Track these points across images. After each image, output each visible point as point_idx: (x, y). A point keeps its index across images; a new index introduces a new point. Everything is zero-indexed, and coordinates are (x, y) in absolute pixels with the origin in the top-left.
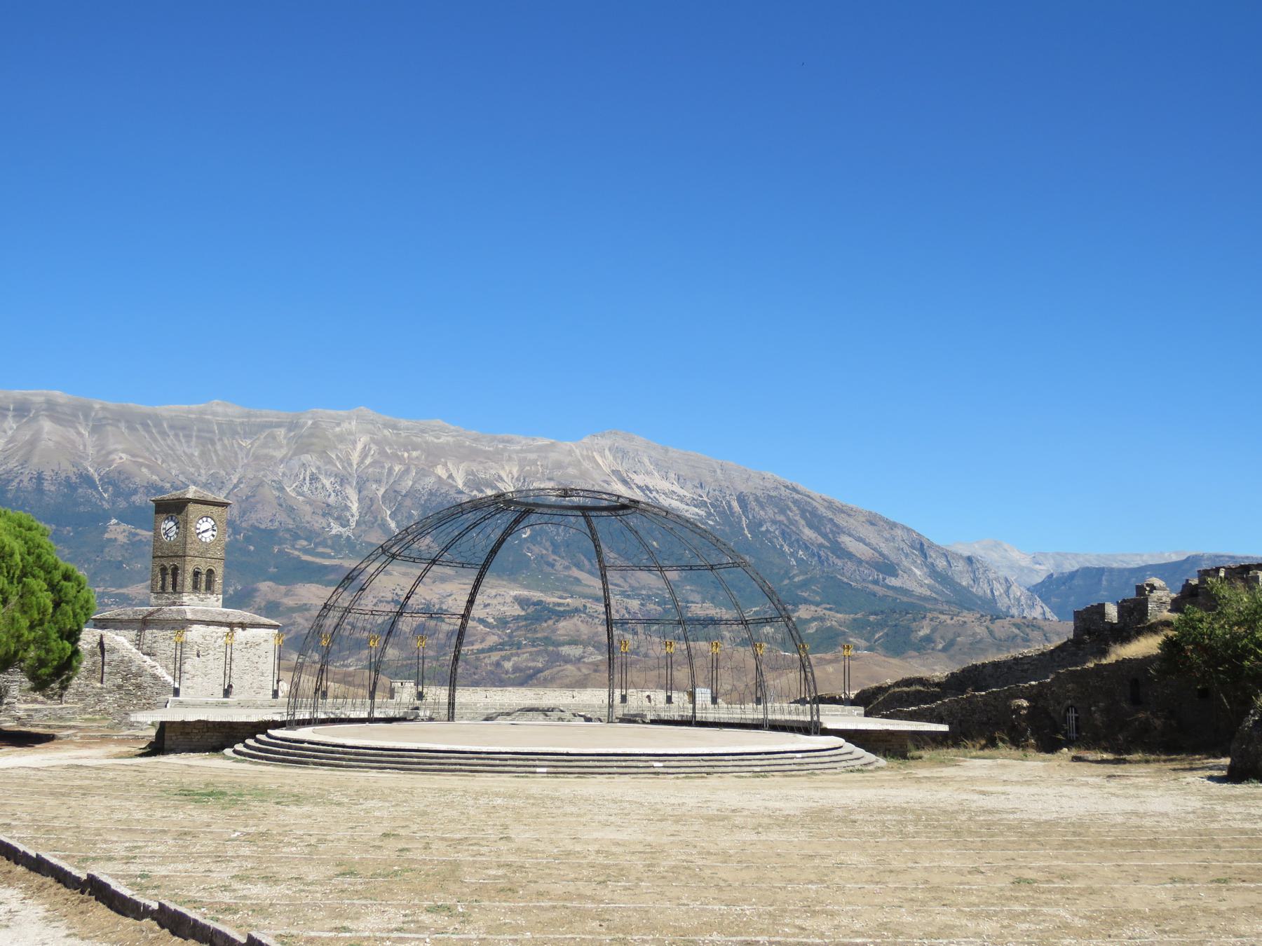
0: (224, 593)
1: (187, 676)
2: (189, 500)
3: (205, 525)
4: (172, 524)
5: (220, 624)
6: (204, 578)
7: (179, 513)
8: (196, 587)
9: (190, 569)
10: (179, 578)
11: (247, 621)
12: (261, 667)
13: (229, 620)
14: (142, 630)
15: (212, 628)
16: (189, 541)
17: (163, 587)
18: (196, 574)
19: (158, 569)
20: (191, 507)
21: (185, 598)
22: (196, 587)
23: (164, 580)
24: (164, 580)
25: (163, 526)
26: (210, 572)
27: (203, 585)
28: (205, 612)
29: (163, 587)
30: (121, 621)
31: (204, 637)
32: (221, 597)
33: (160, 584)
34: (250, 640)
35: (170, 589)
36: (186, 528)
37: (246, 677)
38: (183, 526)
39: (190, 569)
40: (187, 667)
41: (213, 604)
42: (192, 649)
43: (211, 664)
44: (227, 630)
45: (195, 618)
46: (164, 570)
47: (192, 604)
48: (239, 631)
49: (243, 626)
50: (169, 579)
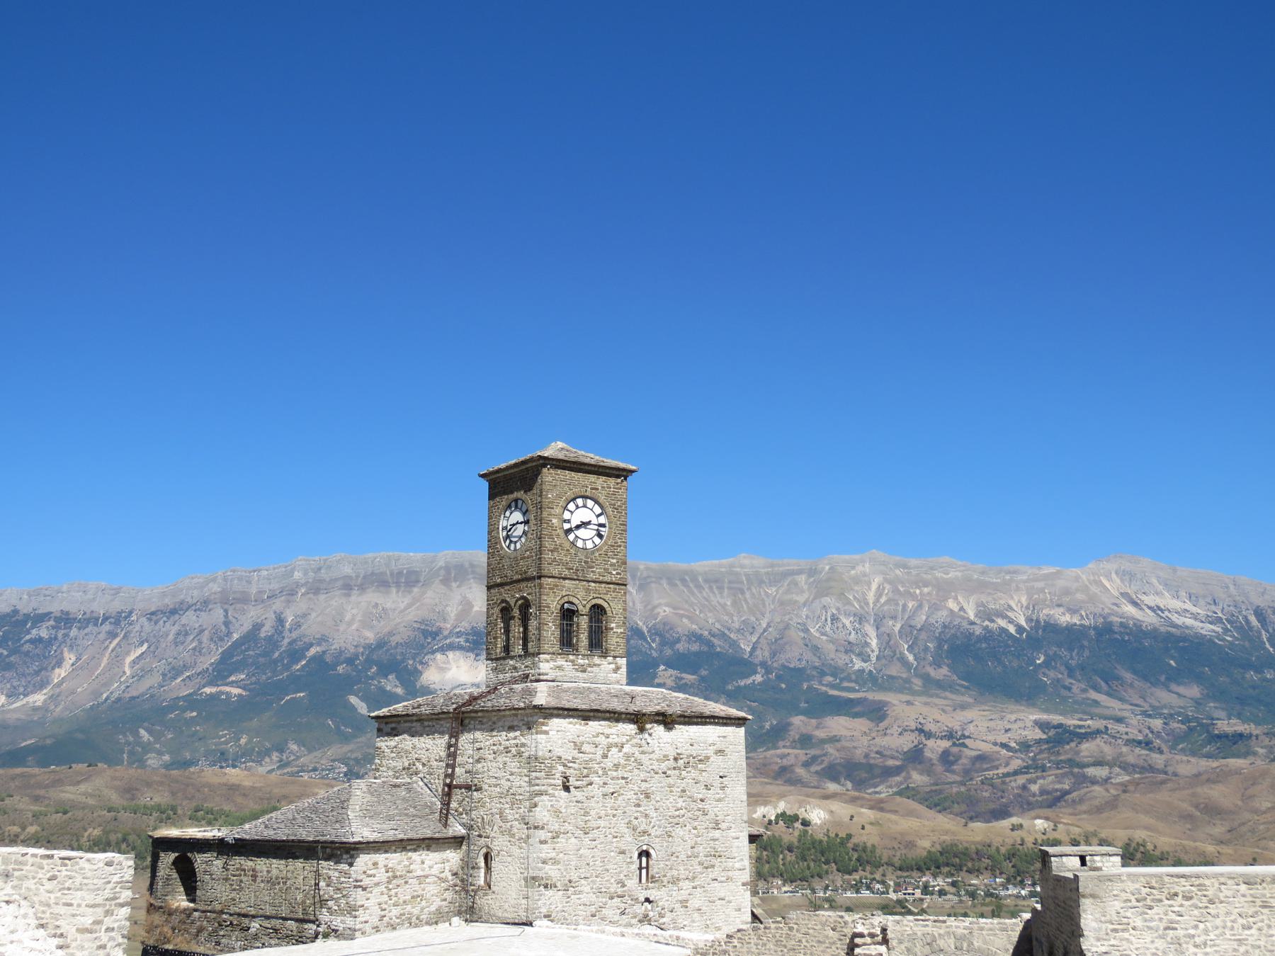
0: (628, 655)
1: (542, 834)
2: (545, 462)
3: (583, 513)
4: (517, 516)
5: (614, 716)
6: (584, 622)
7: (528, 489)
8: (567, 642)
9: (553, 603)
10: (533, 624)
11: (676, 709)
12: (714, 809)
13: (633, 708)
14: (455, 735)
15: (595, 726)
16: (548, 544)
17: (507, 649)
18: (568, 614)
19: (497, 610)
20: (548, 475)
21: (546, 666)
22: (567, 642)
23: (507, 631)
24: (507, 631)
25: (503, 523)
26: (598, 612)
27: (584, 638)
28: (581, 692)
29: (507, 649)
30: (420, 719)
31: (578, 747)
32: (623, 662)
33: (500, 644)
34: (685, 750)
35: (518, 649)
36: (540, 520)
37: (679, 831)
38: (536, 518)
39: (553, 603)
40: (541, 814)
41: (607, 677)
42: (549, 775)
43: (596, 807)
44: (631, 728)
45: (554, 703)
46: (506, 611)
47: (557, 675)
48: (659, 730)
49: (667, 720)
50: (517, 629)
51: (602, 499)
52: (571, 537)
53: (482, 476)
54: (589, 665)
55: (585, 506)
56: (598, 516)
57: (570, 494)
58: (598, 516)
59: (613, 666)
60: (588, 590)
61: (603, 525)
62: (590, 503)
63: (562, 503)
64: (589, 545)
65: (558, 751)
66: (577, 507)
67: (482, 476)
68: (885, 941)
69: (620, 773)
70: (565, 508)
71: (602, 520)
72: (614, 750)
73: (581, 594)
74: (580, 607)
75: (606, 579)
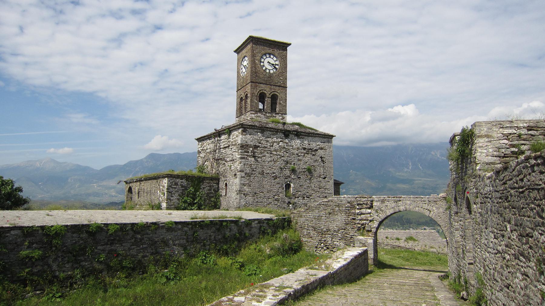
51: (276, 55)
52: (264, 68)
53: (235, 52)
54: (271, 117)
55: (270, 57)
56: (275, 61)
57: (263, 52)
58: (275, 61)
59: (281, 117)
60: (271, 89)
61: (278, 65)
62: (272, 56)
63: (260, 55)
64: (272, 72)
65: (249, 143)
66: (267, 57)
67: (235, 52)
68: (371, 207)
69: (278, 153)
70: (262, 57)
71: (277, 63)
72: (275, 144)
73: (268, 89)
74: (267, 95)
75: (278, 84)
